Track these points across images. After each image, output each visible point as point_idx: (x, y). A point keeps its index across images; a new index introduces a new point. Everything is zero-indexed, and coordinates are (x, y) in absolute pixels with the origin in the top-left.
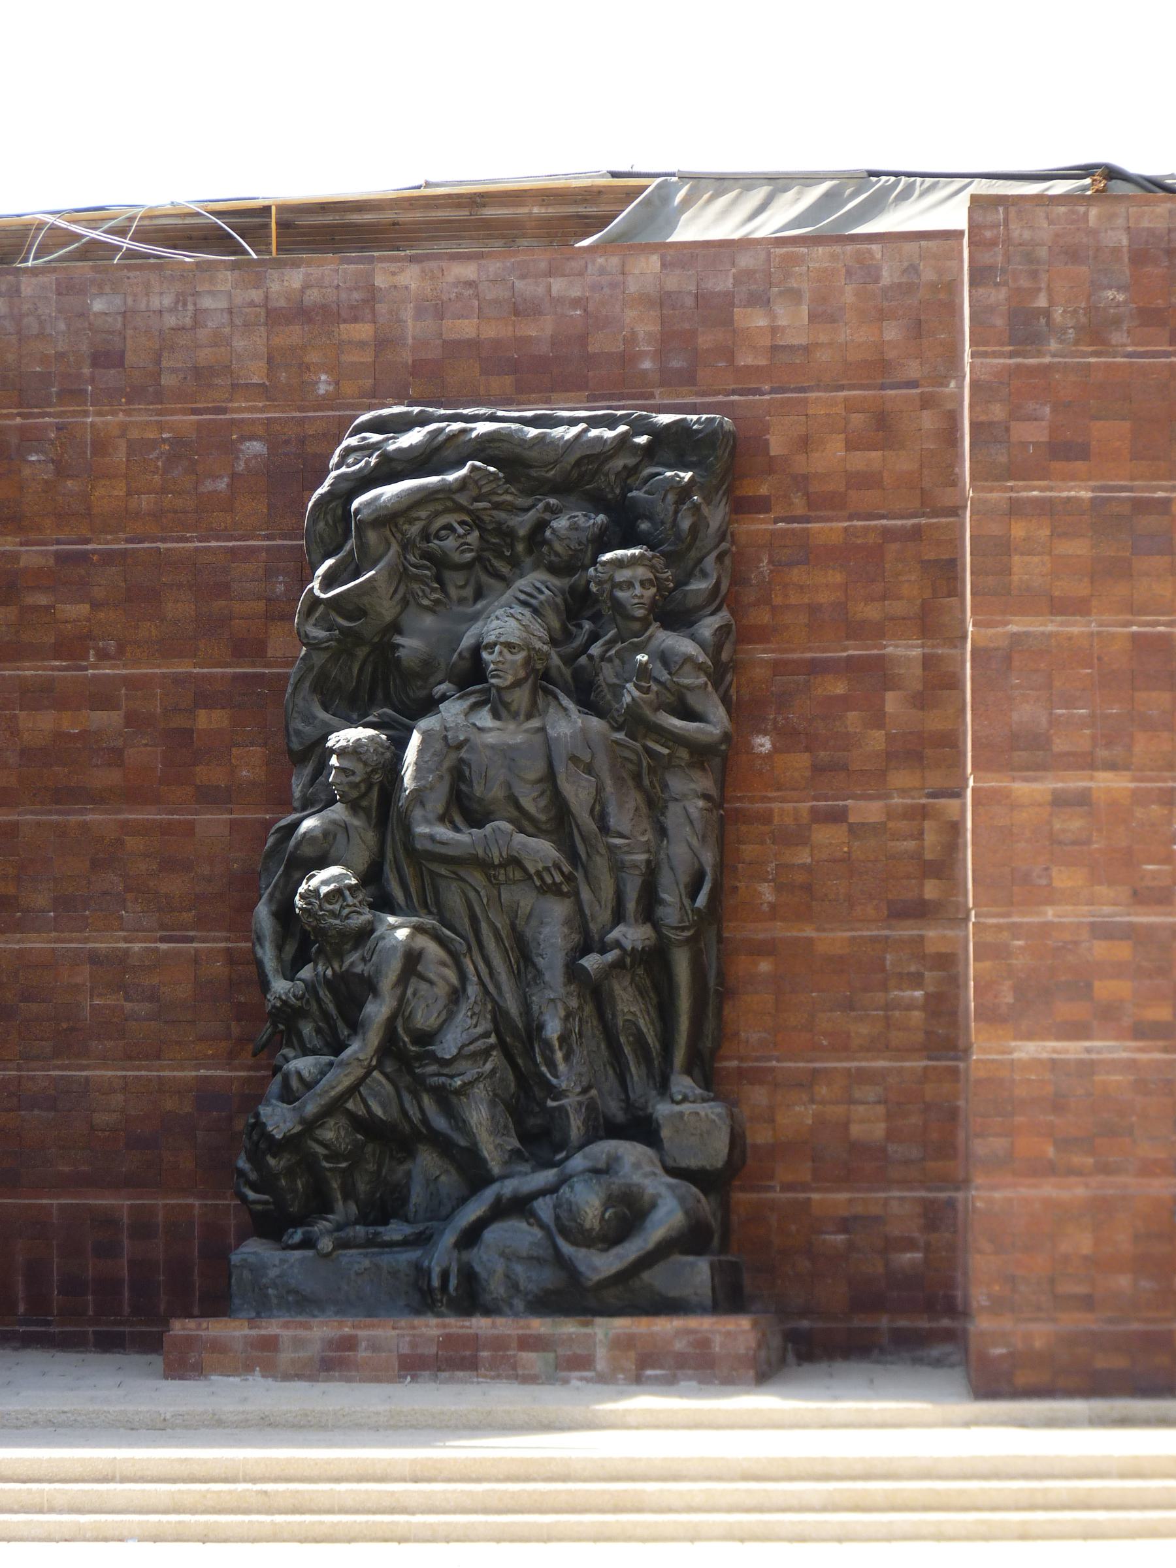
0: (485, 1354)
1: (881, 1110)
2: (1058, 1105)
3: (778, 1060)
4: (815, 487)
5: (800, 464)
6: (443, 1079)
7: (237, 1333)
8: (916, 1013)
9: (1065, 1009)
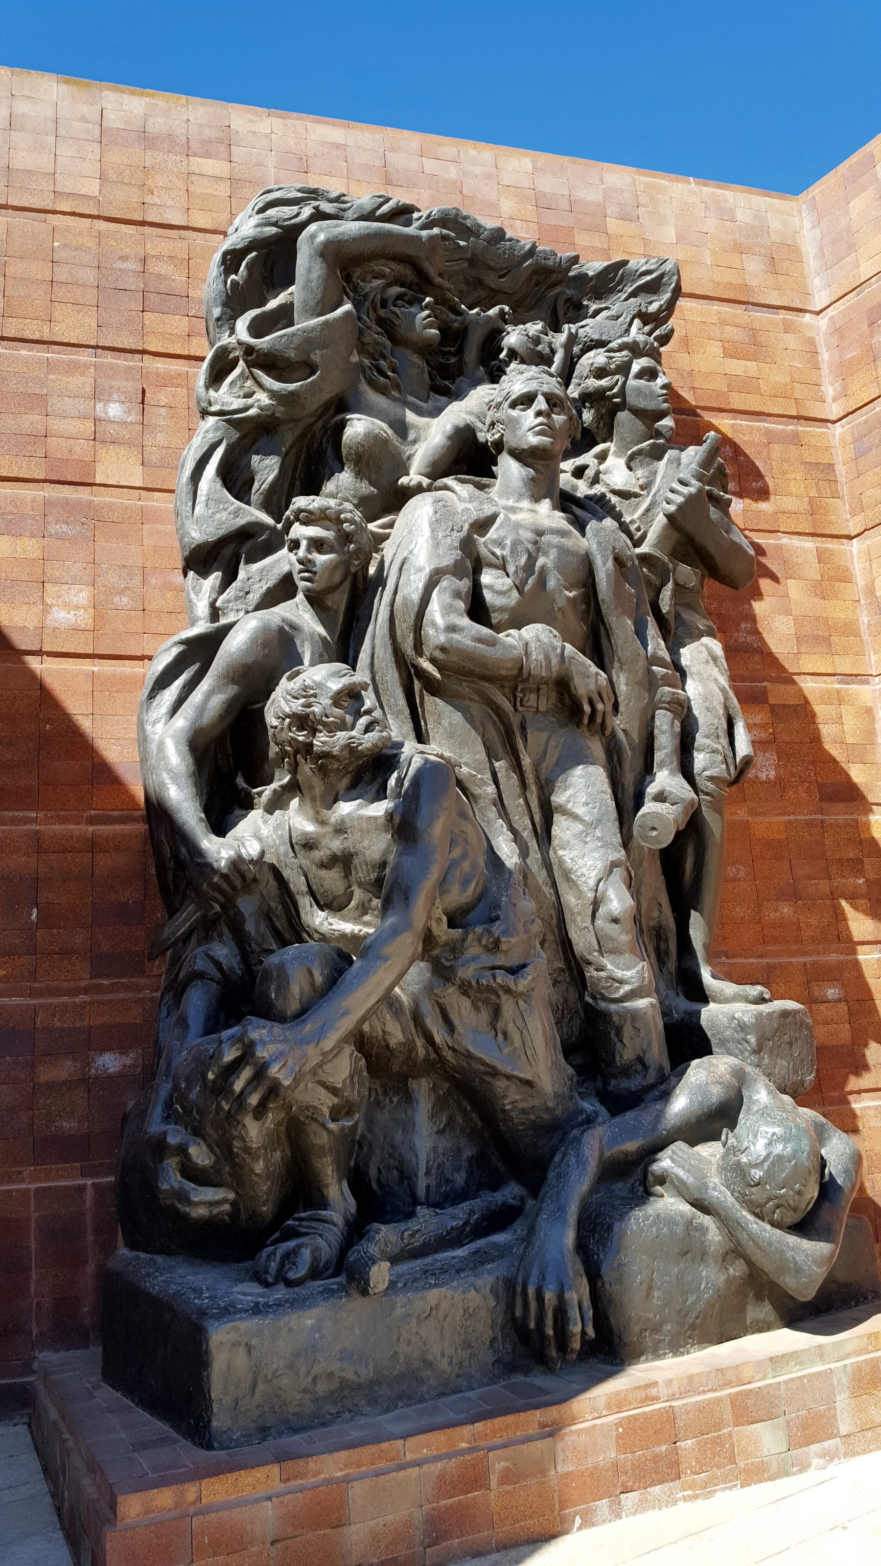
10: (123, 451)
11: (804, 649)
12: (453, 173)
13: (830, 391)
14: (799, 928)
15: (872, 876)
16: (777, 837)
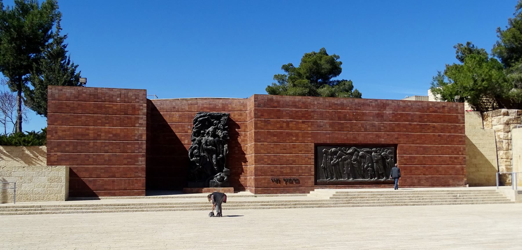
2: (261, 170)
9: (262, 162)
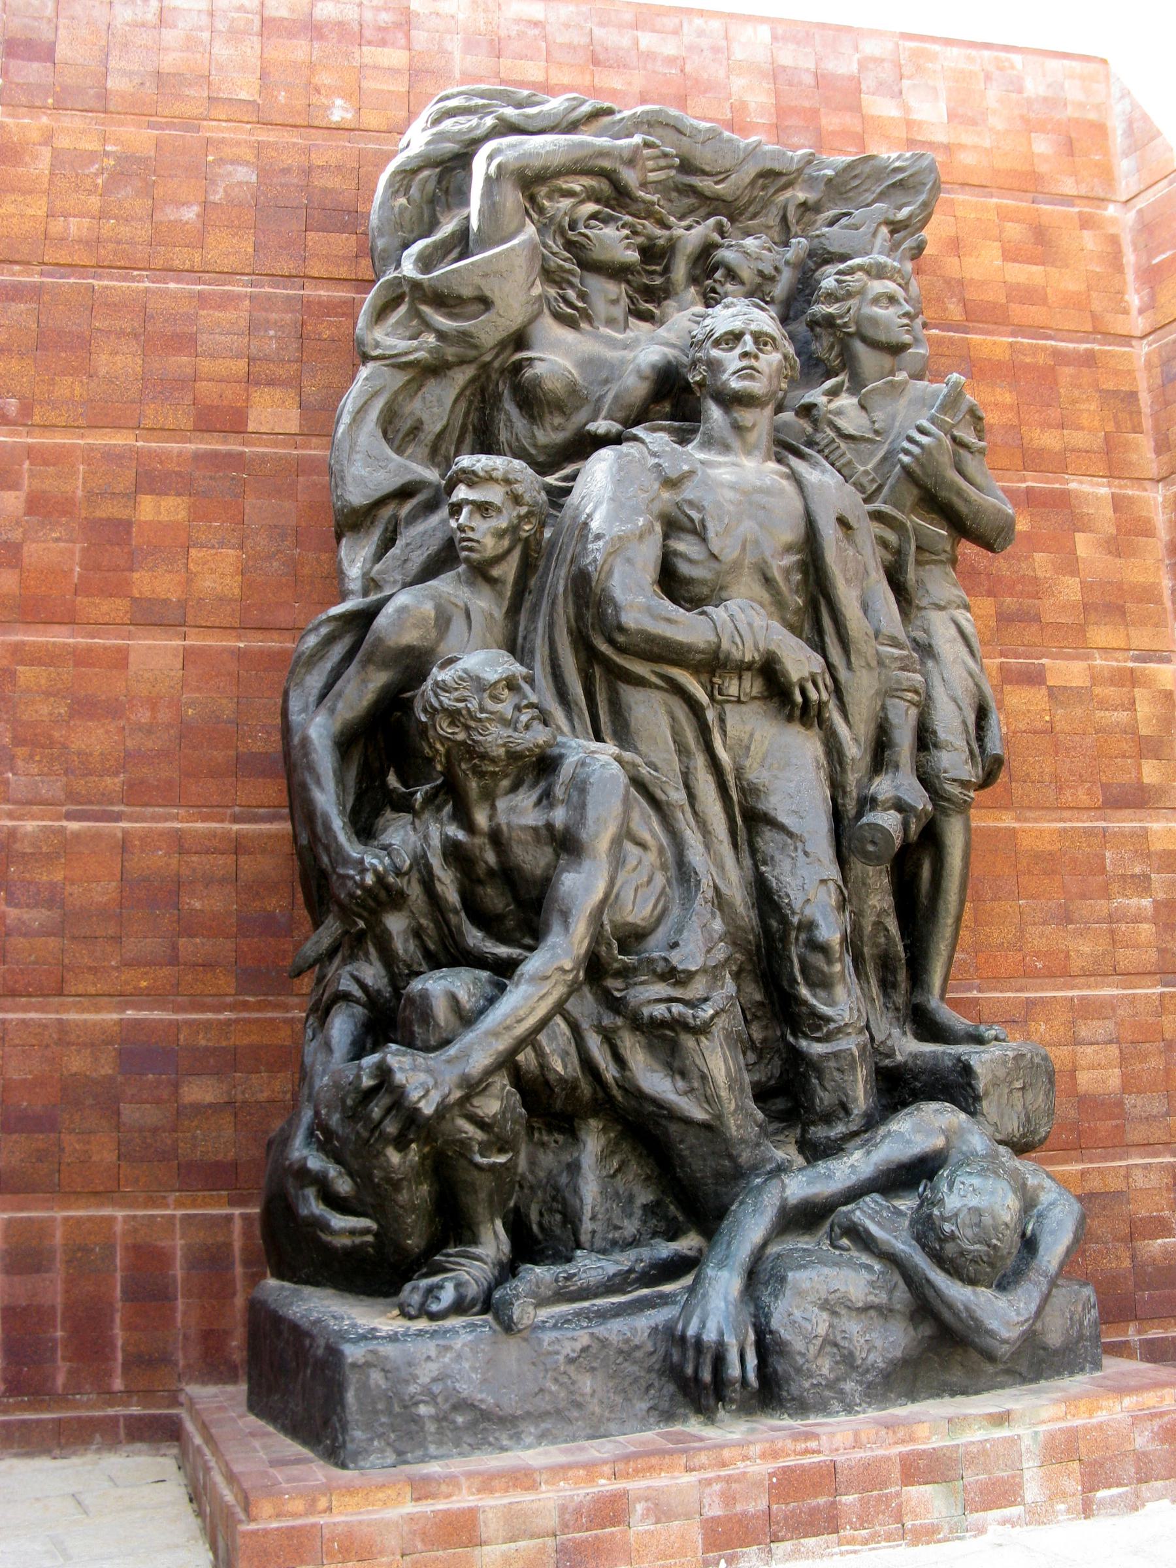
0: (848, 1499)
1: (1113, 1050)
3: (980, 991)
4: (972, 295)
5: (952, 266)
6: (677, 1008)
7: (393, 1513)
8: (1146, 926)
10: (278, 393)
11: (1093, 617)
12: (670, 48)
13: (1134, 300)
14: (1067, 957)
15: (1161, 896)
16: (1049, 848)
